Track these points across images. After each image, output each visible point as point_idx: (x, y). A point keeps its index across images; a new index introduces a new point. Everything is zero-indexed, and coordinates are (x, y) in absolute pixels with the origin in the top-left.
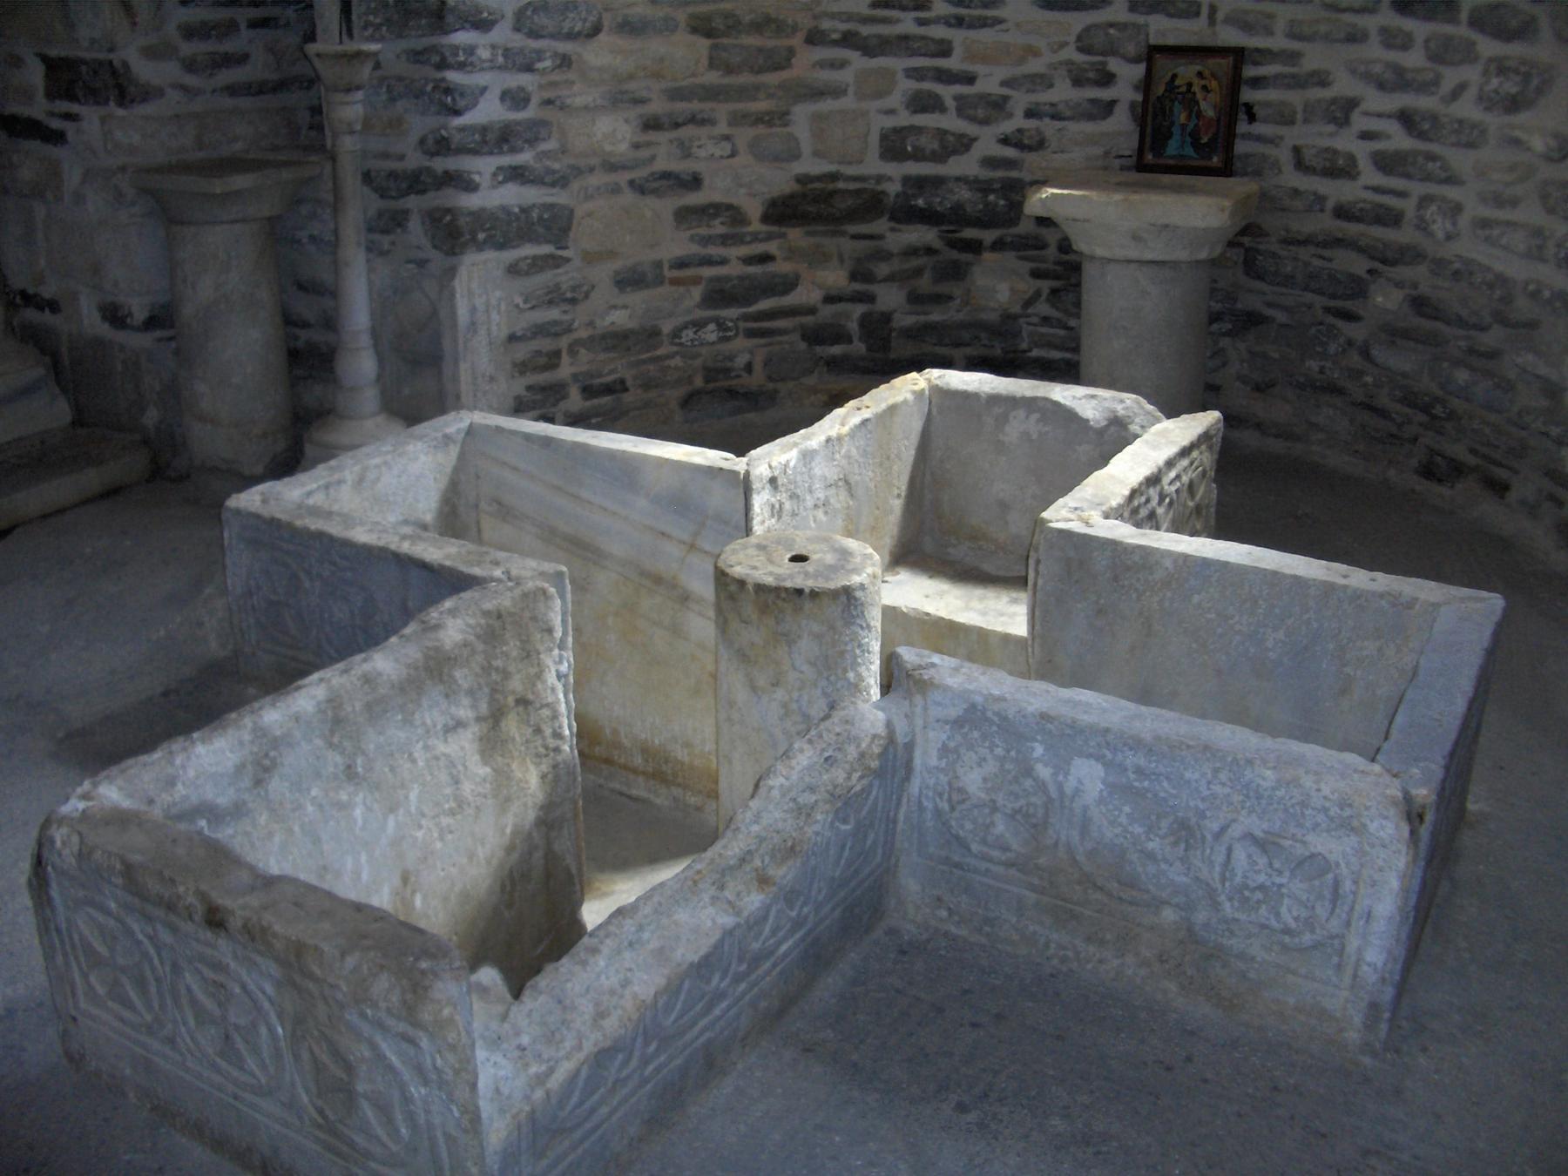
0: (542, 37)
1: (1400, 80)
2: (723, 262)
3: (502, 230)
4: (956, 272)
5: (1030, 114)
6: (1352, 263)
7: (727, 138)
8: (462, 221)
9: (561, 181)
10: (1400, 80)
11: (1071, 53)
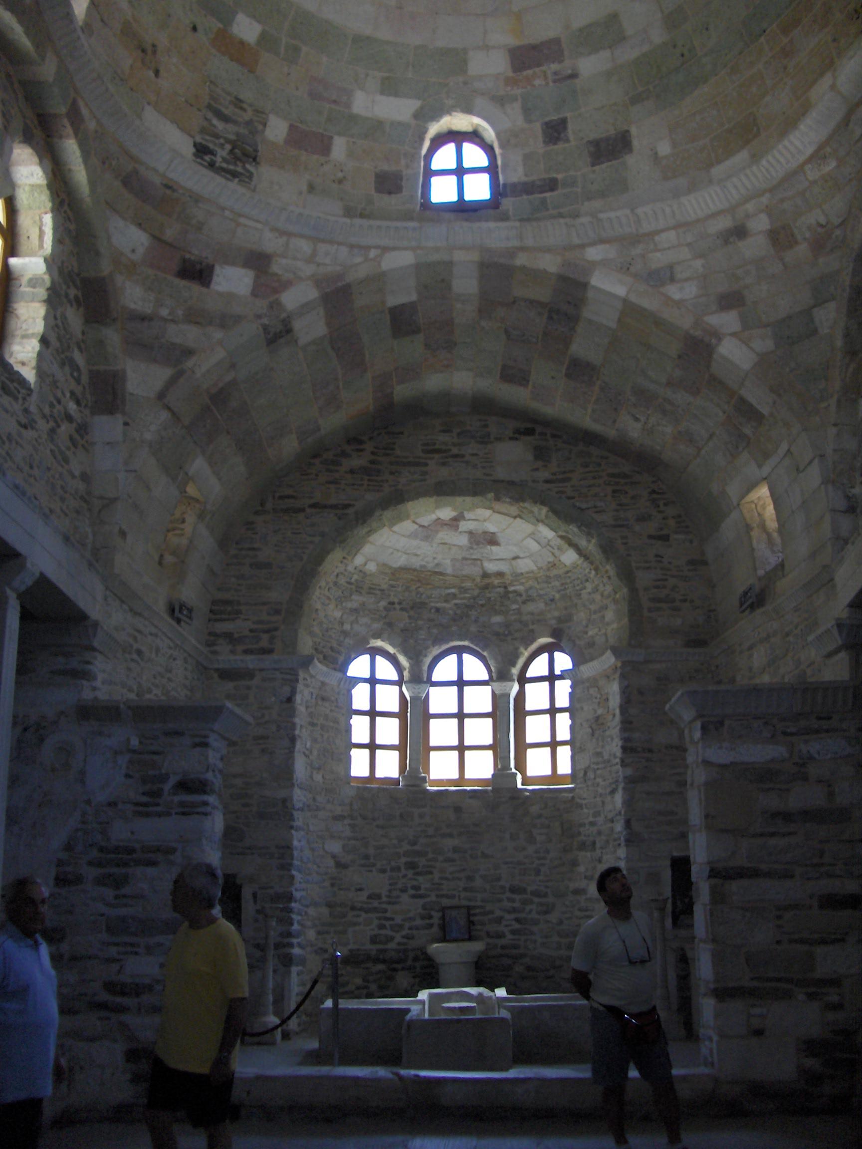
1: (514, 910)
4: (390, 978)
5: (410, 928)
11: (420, 910)
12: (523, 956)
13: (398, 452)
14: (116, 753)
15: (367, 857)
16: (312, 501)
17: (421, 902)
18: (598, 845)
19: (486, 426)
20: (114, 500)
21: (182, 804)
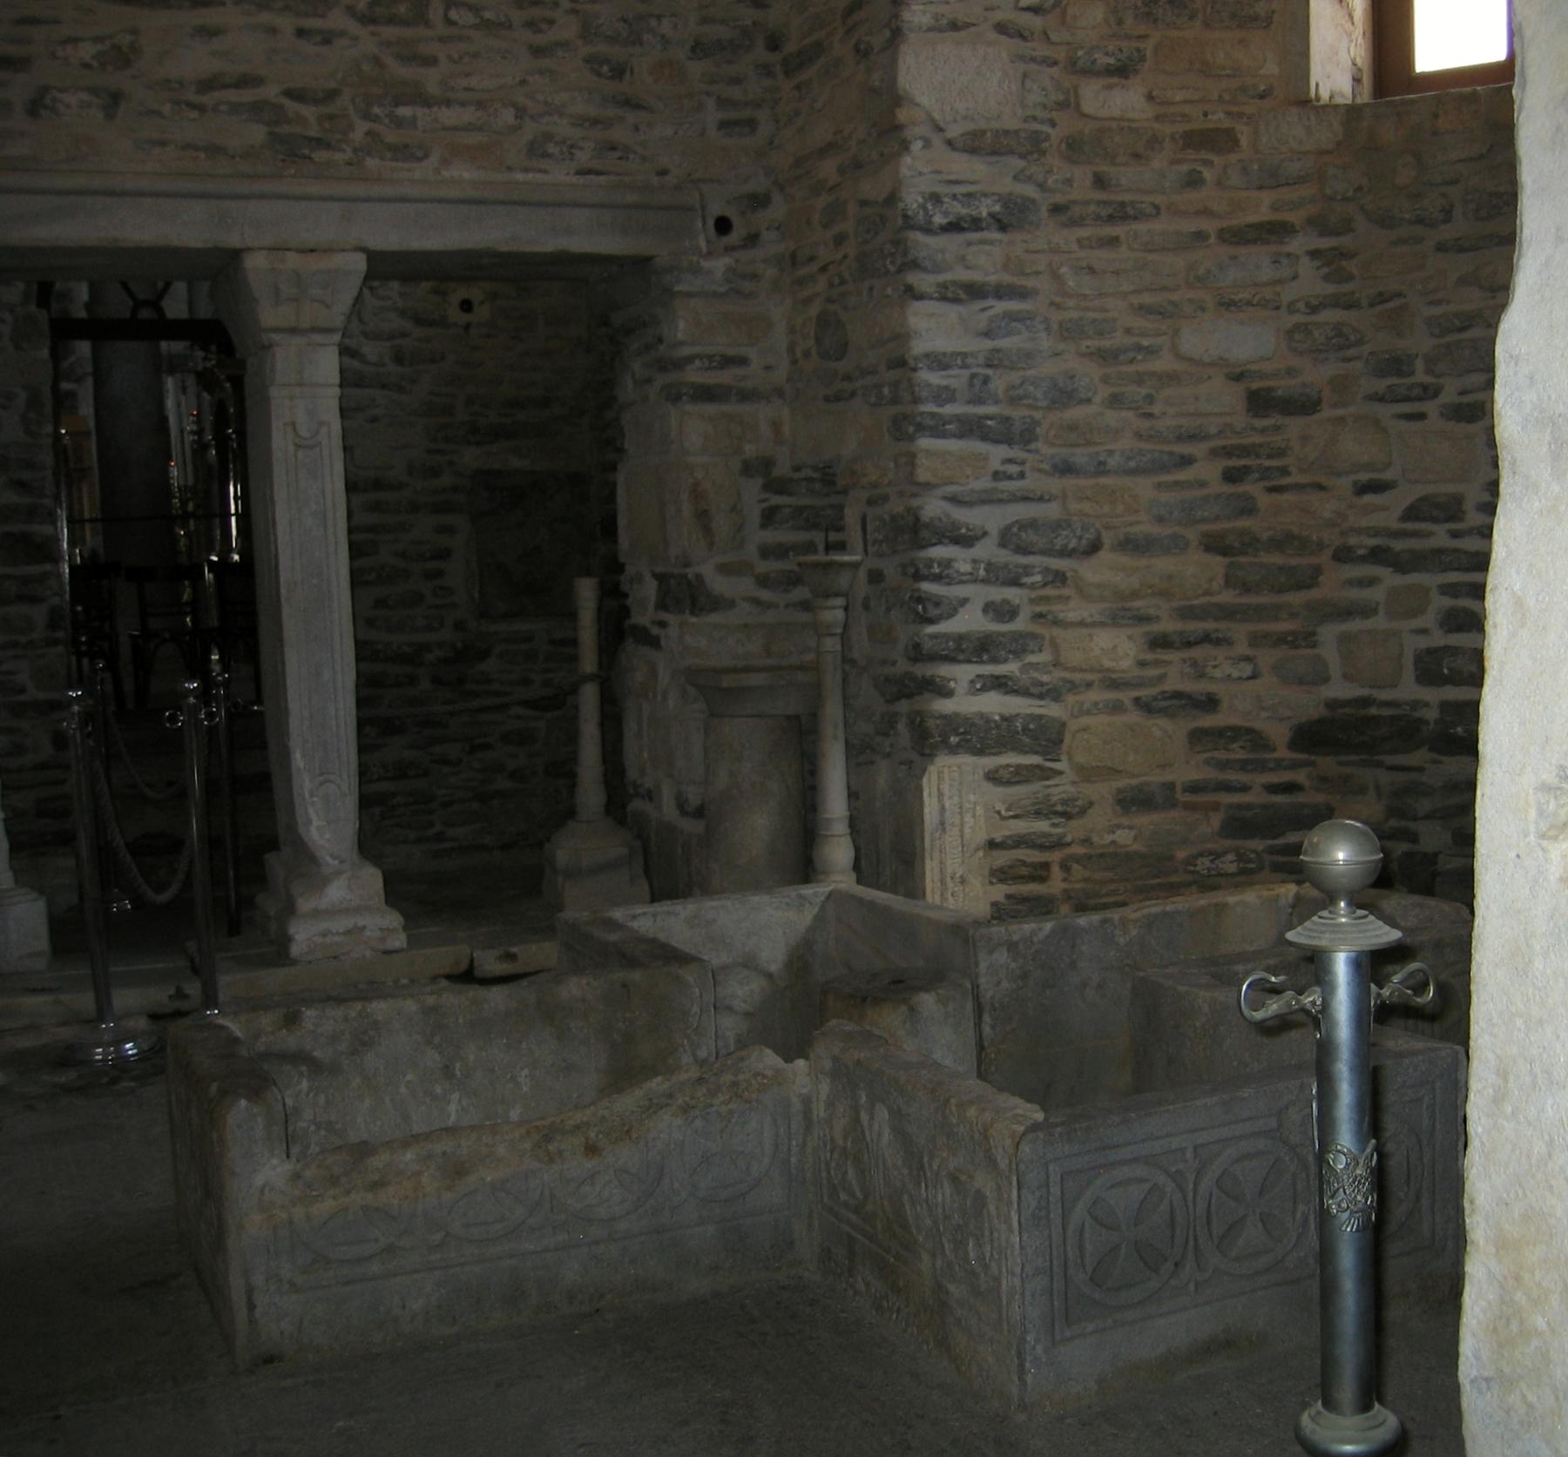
0: (1032, 553)
2: (1244, 789)
3: (977, 737)
7: (1248, 659)
8: (931, 723)
9: (1052, 694)
15: (1397, 365)
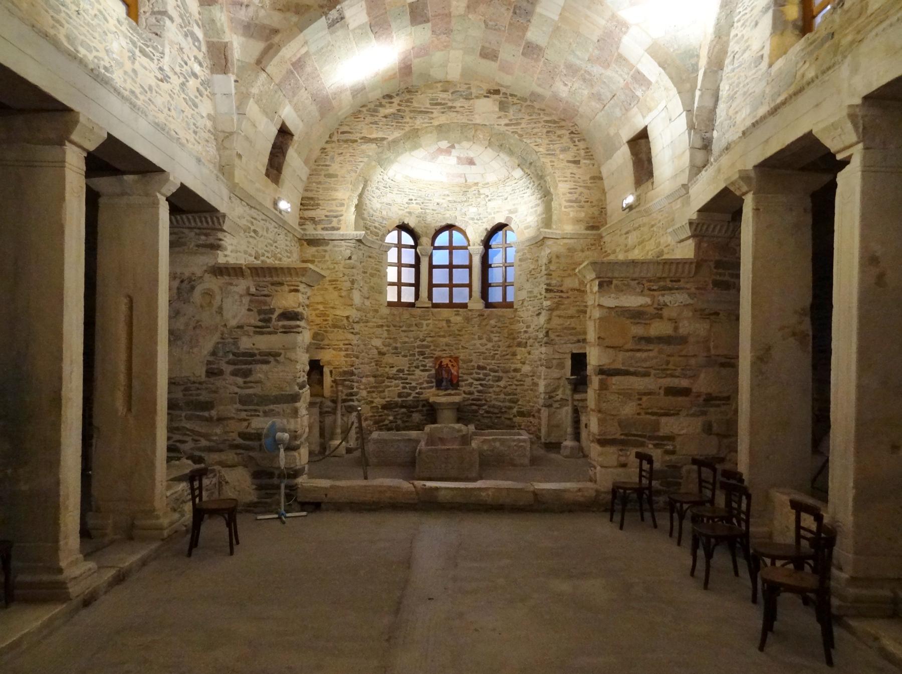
1: (479, 379)
6: (474, 407)
10: (479, 379)
12: (484, 405)
13: (415, 104)
14: (241, 296)
15: (396, 348)
16: (362, 135)
17: (427, 373)
18: (528, 344)
19: (469, 88)
20: (231, 134)
21: (284, 327)
